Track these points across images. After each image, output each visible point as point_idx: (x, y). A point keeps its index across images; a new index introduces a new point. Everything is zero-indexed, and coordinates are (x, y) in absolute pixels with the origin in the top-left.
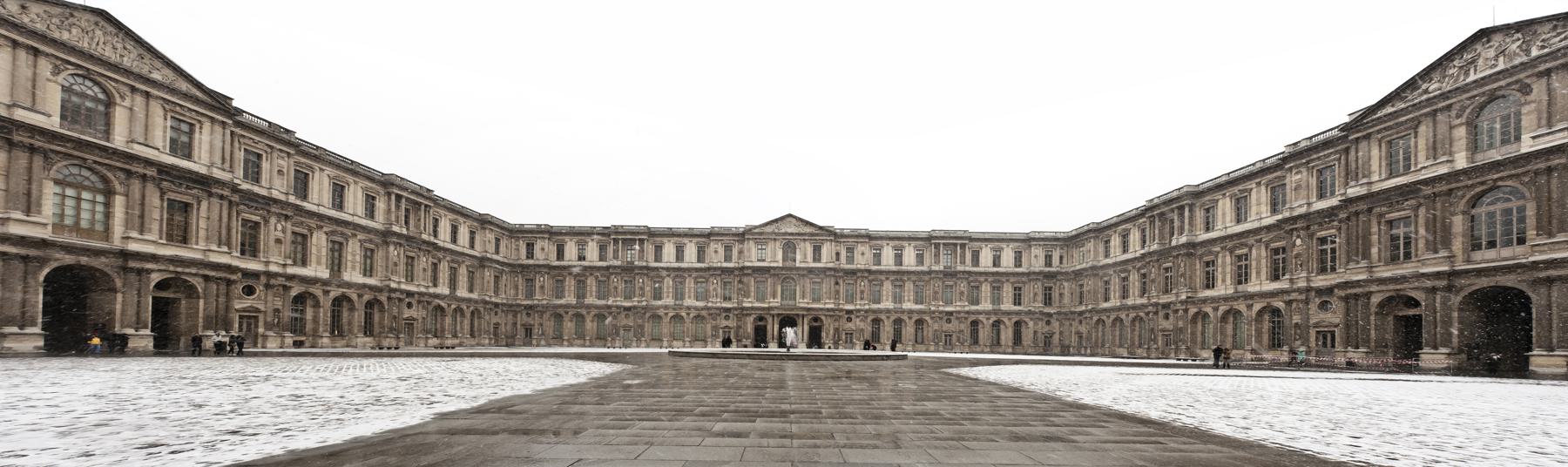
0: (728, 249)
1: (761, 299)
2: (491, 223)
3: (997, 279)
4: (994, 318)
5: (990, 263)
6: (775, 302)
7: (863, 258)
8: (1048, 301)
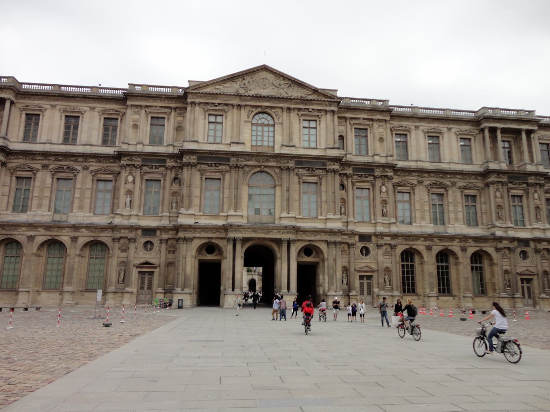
0: (157, 121)
7: (380, 147)
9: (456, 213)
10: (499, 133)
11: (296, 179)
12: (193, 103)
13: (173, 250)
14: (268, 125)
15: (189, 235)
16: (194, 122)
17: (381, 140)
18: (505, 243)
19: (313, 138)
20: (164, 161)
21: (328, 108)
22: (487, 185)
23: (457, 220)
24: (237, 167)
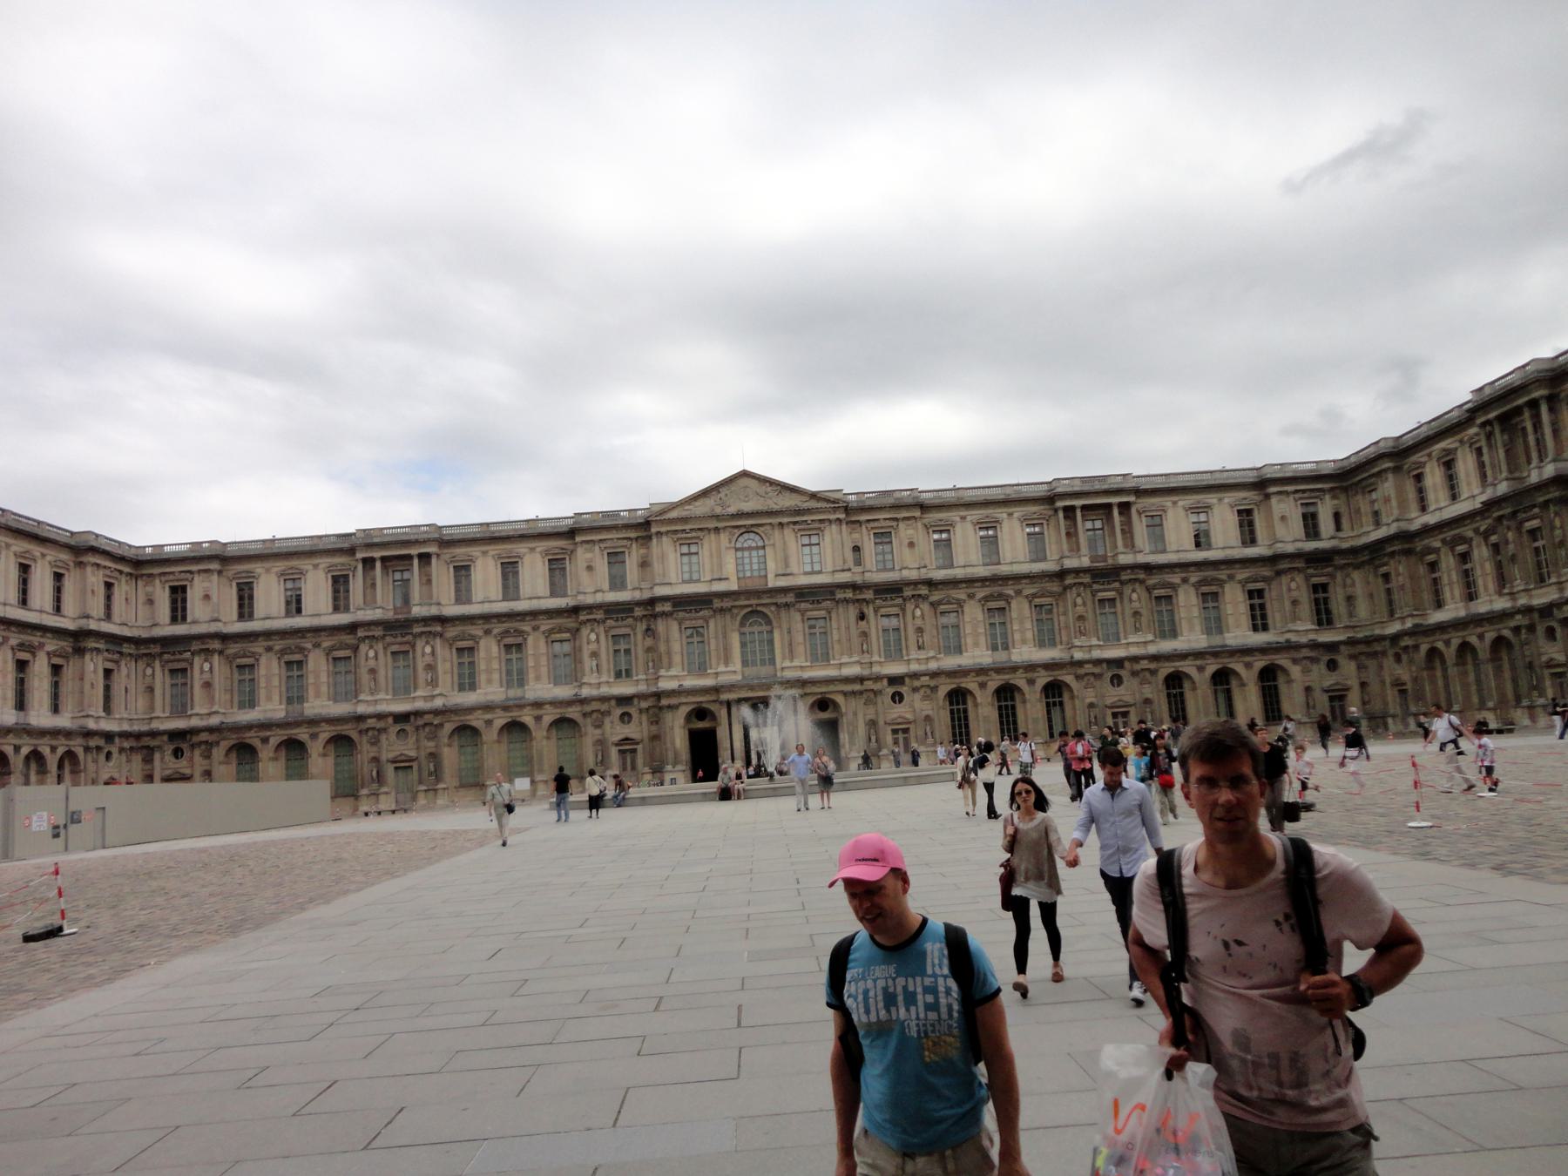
0: (615, 558)
2: (93, 550)
4: (1212, 668)
5: (1189, 542)
7: (911, 556)
8: (1324, 616)
9: (1023, 631)
10: (1079, 513)
11: (798, 616)
12: (659, 533)
13: (656, 721)
14: (757, 548)
15: (674, 701)
16: (663, 557)
17: (911, 545)
18: (1089, 668)
19: (816, 558)
20: (632, 610)
21: (832, 517)
22: (1065, 588)
23: (1024, 642)
24: (722, 610)
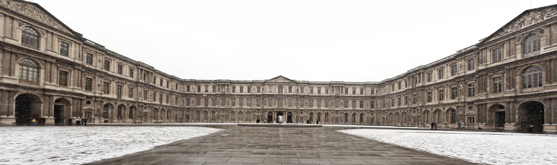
0: (259, 88)
1: (270, 106)
2: (174, 79)
3: (354, 99)
4: (353, 112)
5: (352, 93)
6: (275, 107)
7: (307, 91)
8: (372, 106)
